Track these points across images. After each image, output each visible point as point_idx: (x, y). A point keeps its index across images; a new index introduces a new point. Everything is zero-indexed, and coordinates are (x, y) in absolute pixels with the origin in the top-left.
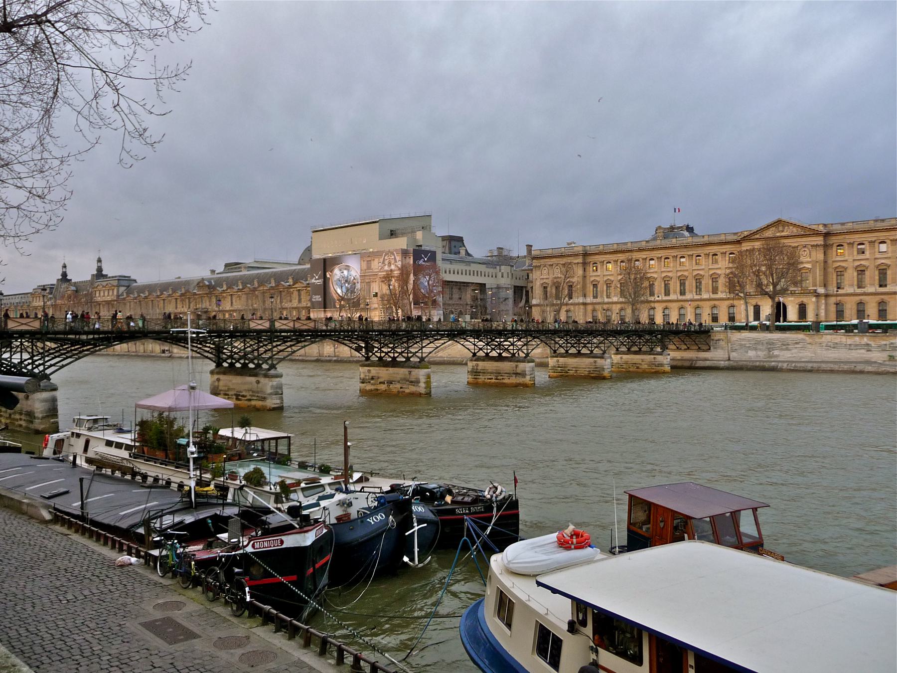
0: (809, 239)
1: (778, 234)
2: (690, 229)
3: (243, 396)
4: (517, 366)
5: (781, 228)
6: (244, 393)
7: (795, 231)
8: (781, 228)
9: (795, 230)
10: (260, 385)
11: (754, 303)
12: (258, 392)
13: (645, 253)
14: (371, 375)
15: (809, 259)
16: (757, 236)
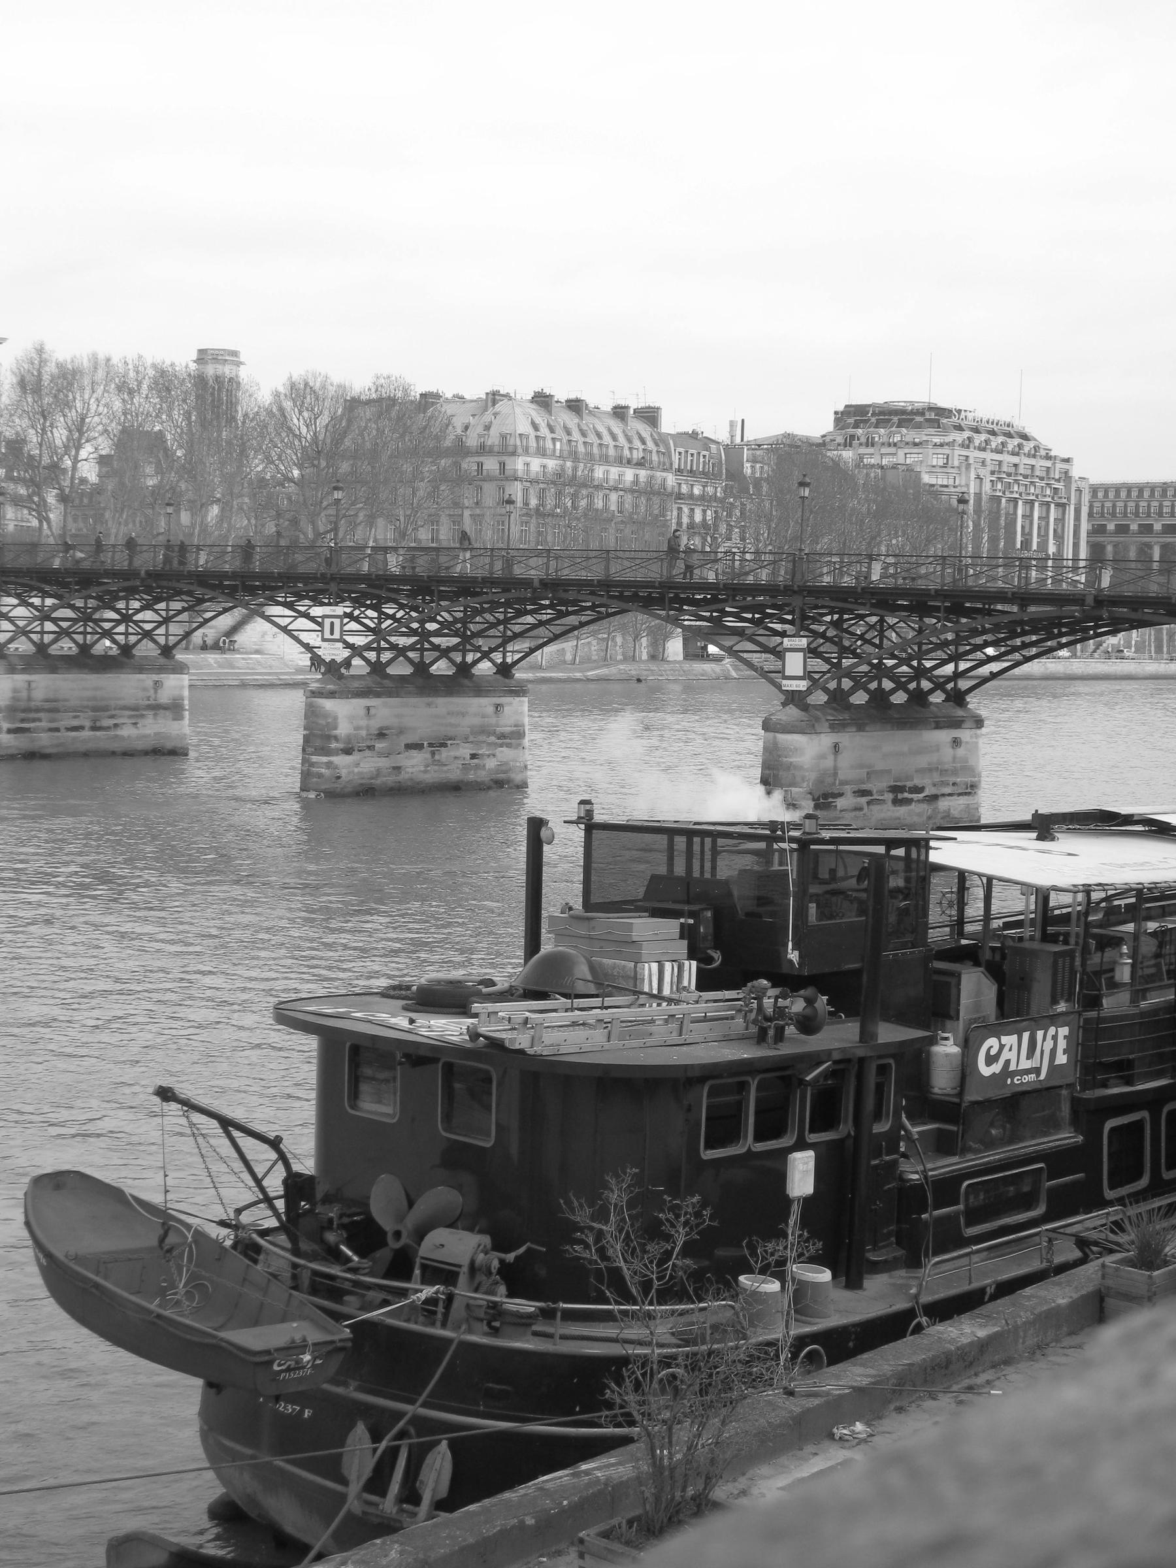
3: (918, 790)
4: (157, 685)
6: (917, 782)
10: (961, 752)
12: (955, 772)
14: (375, 724)
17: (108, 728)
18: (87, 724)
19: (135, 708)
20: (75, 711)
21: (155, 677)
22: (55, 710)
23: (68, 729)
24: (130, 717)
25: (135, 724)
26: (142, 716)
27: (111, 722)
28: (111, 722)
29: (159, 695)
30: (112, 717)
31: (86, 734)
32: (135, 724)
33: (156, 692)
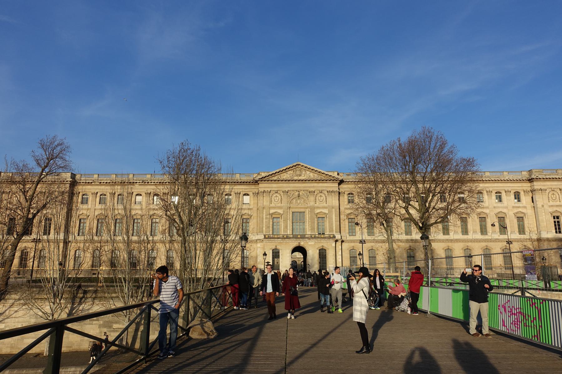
0: (325, 185)
1: (296, 178)
5: (298, 173)
7: (312, 175)
9: (311, 175)
11: (274, 247)
13: (149, 187)
15: (325, 205)
16: (275, 178)
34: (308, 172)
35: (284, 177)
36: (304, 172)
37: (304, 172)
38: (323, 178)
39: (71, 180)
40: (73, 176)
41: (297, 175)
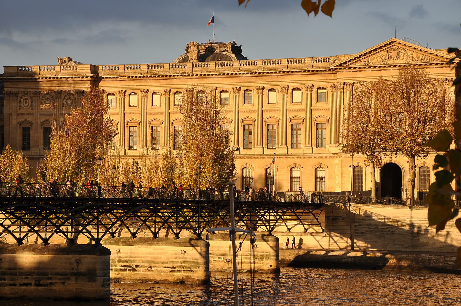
1: (390, 62)
2: (237, 50)
4: (79, 262)
5: (394, 54)
8: (394, 54)
9: (414, 55)
16: (360, 64)
17: (47, 285)
18: (33, 282)
19: (64, 274)
20: (26, 275)
21: (77, 257)
22: (15, 274)
23: (21, 285)
24: (60, 279)
25: (64, 283)
26: (68, 279)
27: (48, 282)
28: (48, 282)
29: (79, 268)
30: (49, 279)
31: (32, 288)
32: (64, 283)
33: (78, 266)
34: (409, 53)
35: (374, 62)
36: (403, 53)
37: (403, 53)
38: (433, 61)
39: (92, 75)
40: (94, 69)
41: (392, 58)
